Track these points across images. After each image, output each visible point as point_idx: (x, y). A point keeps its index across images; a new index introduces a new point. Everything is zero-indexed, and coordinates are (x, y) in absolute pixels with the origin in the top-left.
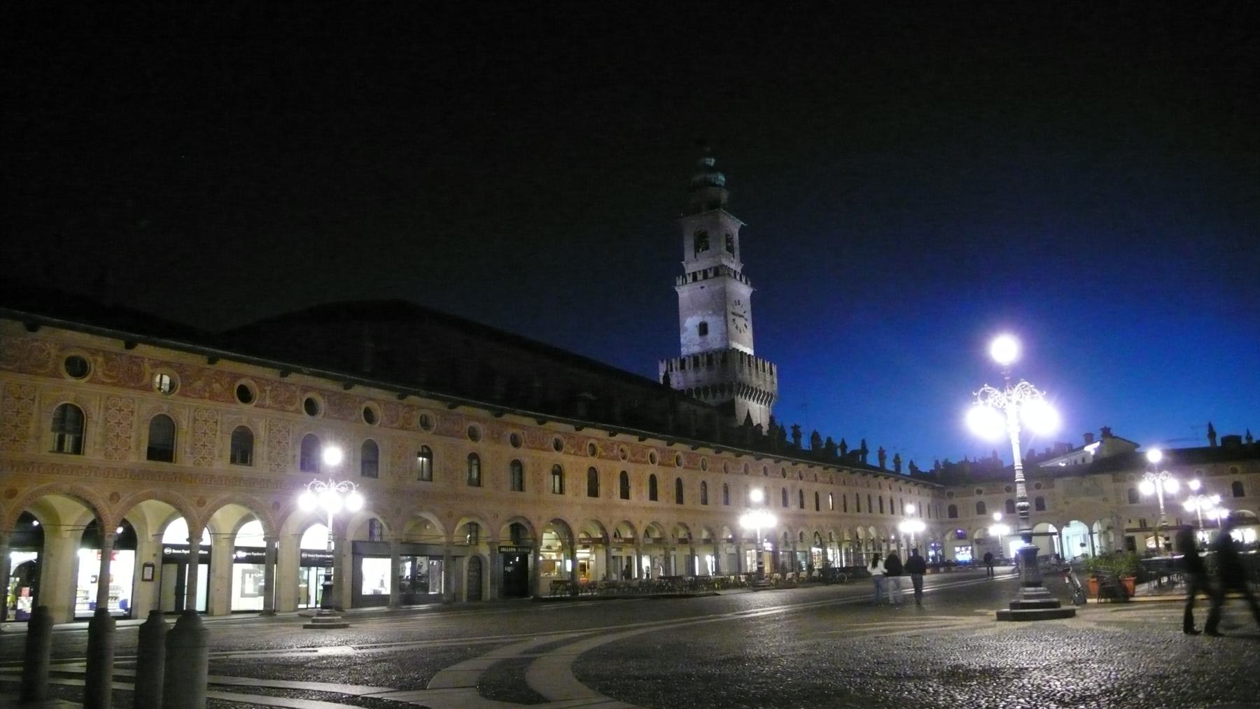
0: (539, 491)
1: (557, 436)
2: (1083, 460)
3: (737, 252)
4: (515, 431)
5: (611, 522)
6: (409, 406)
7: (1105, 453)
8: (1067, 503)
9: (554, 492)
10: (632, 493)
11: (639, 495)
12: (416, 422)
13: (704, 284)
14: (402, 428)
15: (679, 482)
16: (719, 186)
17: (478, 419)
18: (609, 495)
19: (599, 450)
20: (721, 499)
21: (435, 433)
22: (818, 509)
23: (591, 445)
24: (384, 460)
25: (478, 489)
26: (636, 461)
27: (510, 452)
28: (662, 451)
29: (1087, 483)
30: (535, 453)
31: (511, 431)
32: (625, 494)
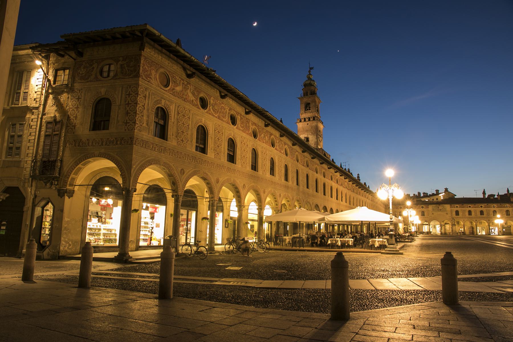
7: (446, 197)
8: (433, 214)
13: (308, 122)
17: (317, 164)
29: (441, 207)
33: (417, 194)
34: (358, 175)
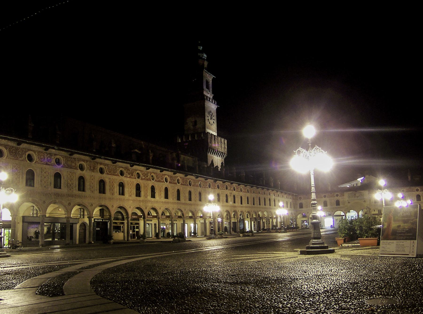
1: (121, 169)
2: (357, 184)
3: (211, 89)
4: (102, 166)
5: (146, 208)
6: (50, 154)
9: (120, 194)
10: (157, 195)
11: (160, 196)
12: (53, 161)
14: (47, 164)
15: (178, 191)
16: (204, 59)
17: (84, 161)
18: (146, 196)
20: (198, 199)
21: (63, 167)
22: (241, 204)
23: (138, 173)
24: (37, 179)
25: (84, 193)
26: (159, 181)
27: (98, 176)
28: (171, 177)
30: (110, 176)
32: (153, 196)
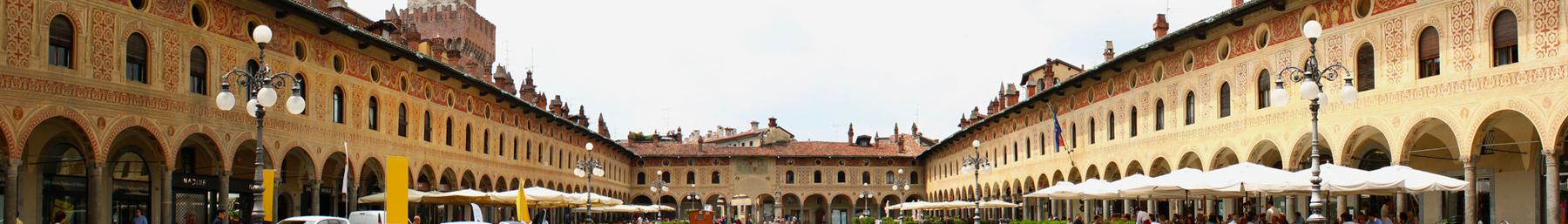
0: (358, 126)
19: (409, 84)
26: (438, 102)
27: (331, 77)
28: (458, 93)
31: (333, 52)
32: (427, 137)
33: (715, 130)
34: (529, 74)
